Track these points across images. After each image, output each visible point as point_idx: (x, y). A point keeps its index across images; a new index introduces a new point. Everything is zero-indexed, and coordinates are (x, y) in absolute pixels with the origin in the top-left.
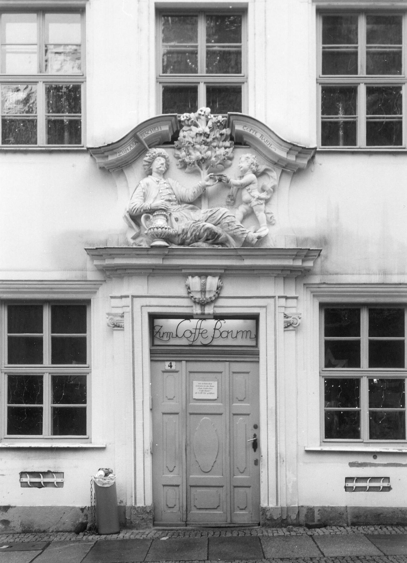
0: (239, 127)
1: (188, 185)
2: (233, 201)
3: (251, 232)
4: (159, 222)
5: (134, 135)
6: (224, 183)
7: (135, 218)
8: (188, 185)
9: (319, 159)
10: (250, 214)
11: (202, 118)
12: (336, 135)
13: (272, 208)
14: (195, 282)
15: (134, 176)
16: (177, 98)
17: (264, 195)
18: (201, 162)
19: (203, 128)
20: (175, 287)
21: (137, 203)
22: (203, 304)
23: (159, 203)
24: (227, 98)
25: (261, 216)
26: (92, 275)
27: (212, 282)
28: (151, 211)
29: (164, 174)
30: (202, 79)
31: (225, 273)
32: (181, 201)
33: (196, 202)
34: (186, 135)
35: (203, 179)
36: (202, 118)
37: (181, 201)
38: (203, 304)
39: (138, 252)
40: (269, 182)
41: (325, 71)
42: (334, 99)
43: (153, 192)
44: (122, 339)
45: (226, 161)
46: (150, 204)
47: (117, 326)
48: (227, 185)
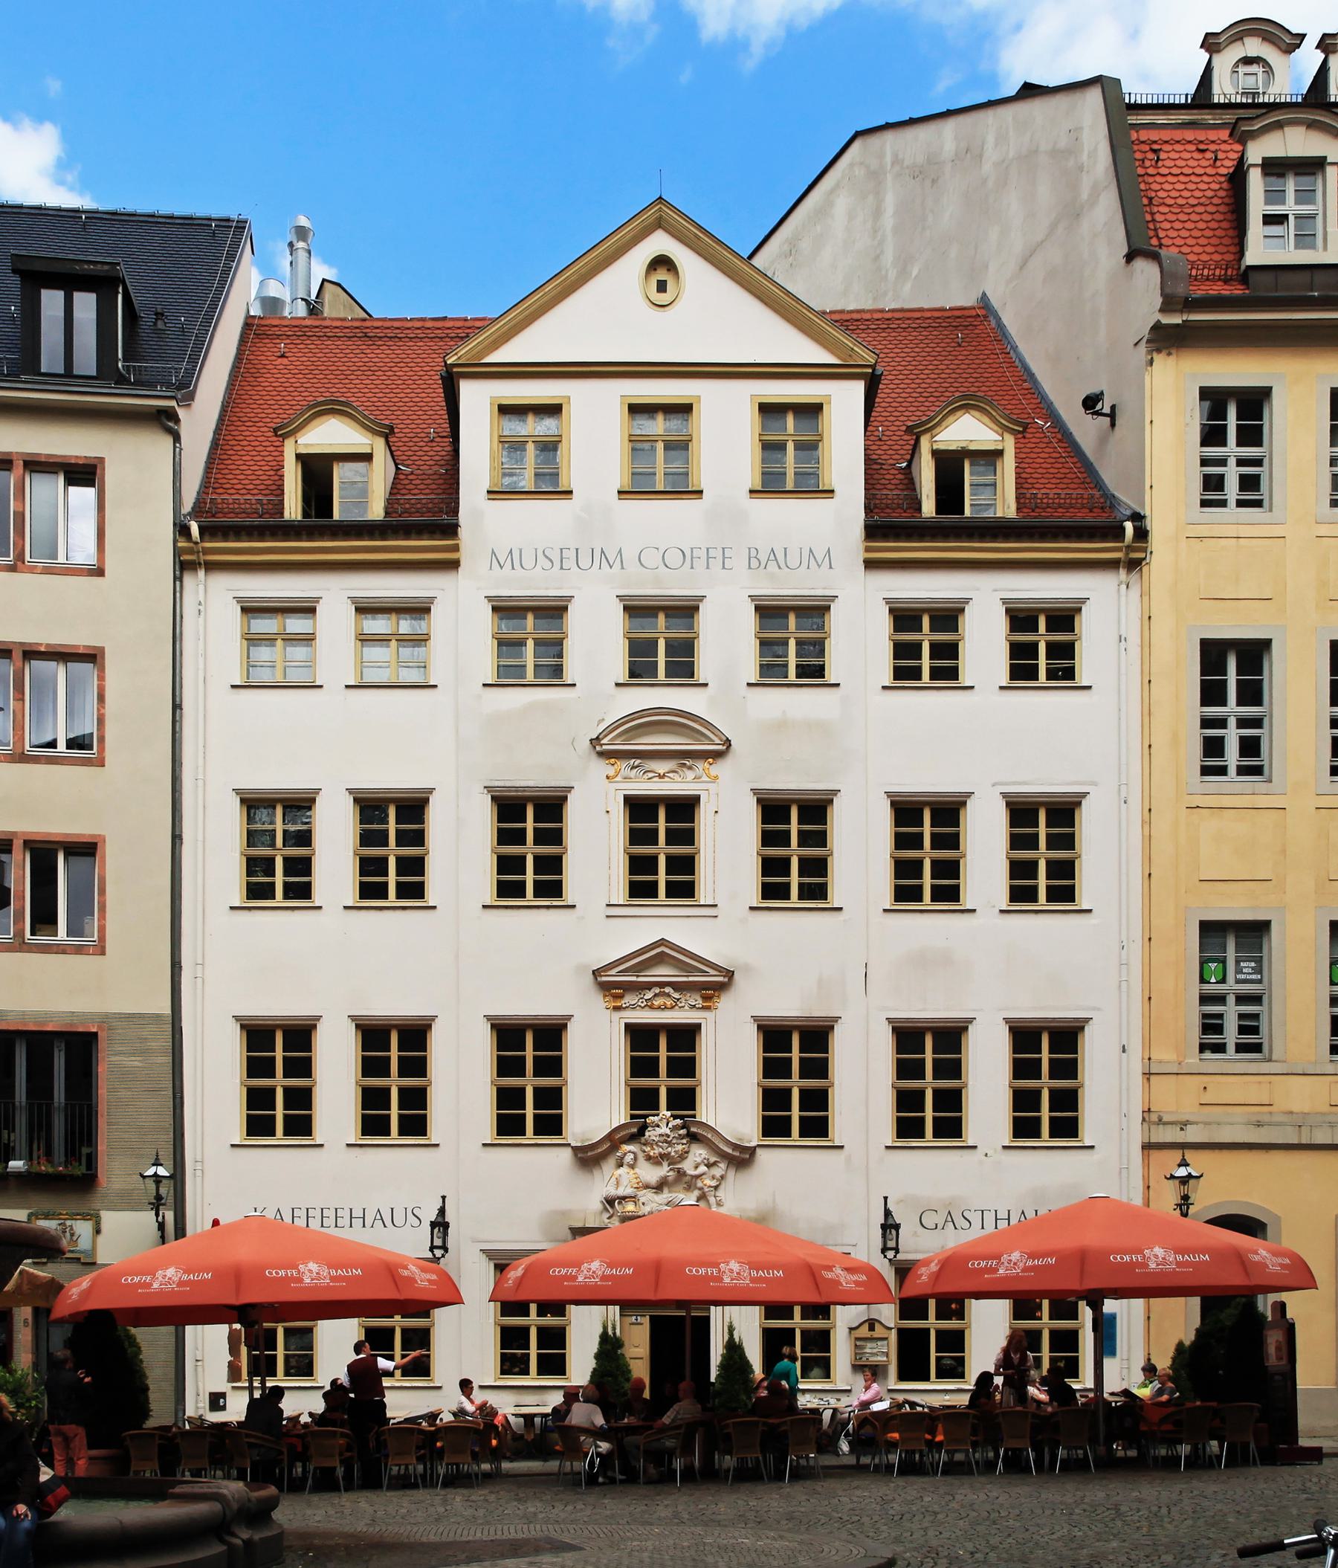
0: (693, 1129)
1: (652, 1174)
2: (689, 1187)
5: (609, 1136)
6: (681, 1173)
7: (610, 1201)
8: (652, 1174)
9: (759, 1151)
10: (703, 1197)
11: (663, 1122)
12: (774, 1127)
13: (720, 1193)
16: (642, 1100)
17: (714, 1183)
18: (662, 1156)
19: (664, 1130)
21: (613, 1191)
23: (629, 1191)
24: (684, 1100)
25: (712, 1200)
28: (624, 1198)
29: (632, 1167)
30: (663, 1083)
32: (647, 1187)
33: (659, 1187)
35: (664, 1170)
36: (663, 1122)
37: (647, 1187)
42: (773, 1100)
43: (624, 1181)
45: (683, 1156)
46: (621, 1192)
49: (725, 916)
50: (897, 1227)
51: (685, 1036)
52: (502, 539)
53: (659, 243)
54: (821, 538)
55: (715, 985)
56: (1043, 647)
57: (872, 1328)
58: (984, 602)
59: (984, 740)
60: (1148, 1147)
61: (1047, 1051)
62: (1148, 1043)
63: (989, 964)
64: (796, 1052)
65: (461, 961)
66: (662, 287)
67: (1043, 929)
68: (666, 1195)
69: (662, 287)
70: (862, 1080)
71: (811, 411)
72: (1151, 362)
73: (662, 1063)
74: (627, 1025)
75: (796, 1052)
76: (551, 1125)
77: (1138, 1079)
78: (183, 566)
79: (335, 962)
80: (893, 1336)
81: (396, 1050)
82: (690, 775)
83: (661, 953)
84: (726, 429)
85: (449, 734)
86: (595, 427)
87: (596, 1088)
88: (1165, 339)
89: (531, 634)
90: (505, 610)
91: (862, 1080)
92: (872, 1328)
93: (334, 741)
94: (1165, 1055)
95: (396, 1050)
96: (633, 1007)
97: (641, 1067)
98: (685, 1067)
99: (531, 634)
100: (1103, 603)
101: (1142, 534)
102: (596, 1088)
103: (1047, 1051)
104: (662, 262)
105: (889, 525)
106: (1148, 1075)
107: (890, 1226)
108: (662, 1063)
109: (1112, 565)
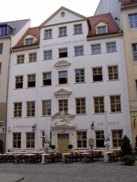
3: (67, 125)
4: (58, 124)
7: (55, 123)
8: (61, 120)
9: (76, 116)
12: (78, 112)
14: (62, 130)
15: (55, 118)
16: (61, 110)
20: (60, 131)
21: (56, 122)
22: (63, 133)
24: (66, 109)
26: (52, 130)
27: (64, 130)
30: (63, 107)
31: (65, 129)
34: (61, 114)
35: (63, 119)
38: (63, 133)
39: (55, 127)
40: (70, 119)
41: (77, 105)
42: (78, 109)
44: (54, 136)
47: (54, 135)
48: (65, 119)
49: (71, 86)
50: (93, 125)
51: (66, 101)
52: (45, 45)
53: (63, 11)
54: (82, 39)
55: (69, 94)
56: (111, 47)
57: (91, 140)
58: (103, 43)
59: (104, 59)
60: (131, 112)
61: (115, 99)
62: (129, 97)
63: (106, 88)
64: (81, 103)
65: (39, 94)
66: (63, 15)
67: (114, 83)
68: (63, 122)
69: (63, 15)
70: (90, 105)
71: (80, 25)
72: (121, 12)
73: (63, 105)
74: (59, 100)
75: (81, 103)
76: (50, 114)
77: (128, 103)
78: (11, 52)
79: (25, 95)
80: (95, 141)
81: (31, 105)
82: (66, 68)
83: (62, 90)
84: (70, 29)
85: (39, 68)
86: (55, 31)
87: (55, 109)
88: (123, 9)
89: (48, 54)
90: (45, 52)
91: (90, 105)
92: (91, 140)
93: (26, 69)
94: (131, 99)
95: (31, 105)
96: (59, 98)
97: (60, 105)
98: (66, 105)
99: (48, 54)
100: (118, 41)
101: (122, 32)
102: (55, 109)
103: (115, 99)
104: (63, 13)
105: (91, 35)
106: (130, 102)
107: (93, 125)
108: (63, 105)
109: (119, 36)
